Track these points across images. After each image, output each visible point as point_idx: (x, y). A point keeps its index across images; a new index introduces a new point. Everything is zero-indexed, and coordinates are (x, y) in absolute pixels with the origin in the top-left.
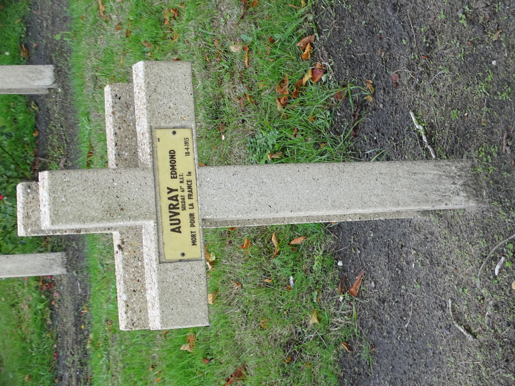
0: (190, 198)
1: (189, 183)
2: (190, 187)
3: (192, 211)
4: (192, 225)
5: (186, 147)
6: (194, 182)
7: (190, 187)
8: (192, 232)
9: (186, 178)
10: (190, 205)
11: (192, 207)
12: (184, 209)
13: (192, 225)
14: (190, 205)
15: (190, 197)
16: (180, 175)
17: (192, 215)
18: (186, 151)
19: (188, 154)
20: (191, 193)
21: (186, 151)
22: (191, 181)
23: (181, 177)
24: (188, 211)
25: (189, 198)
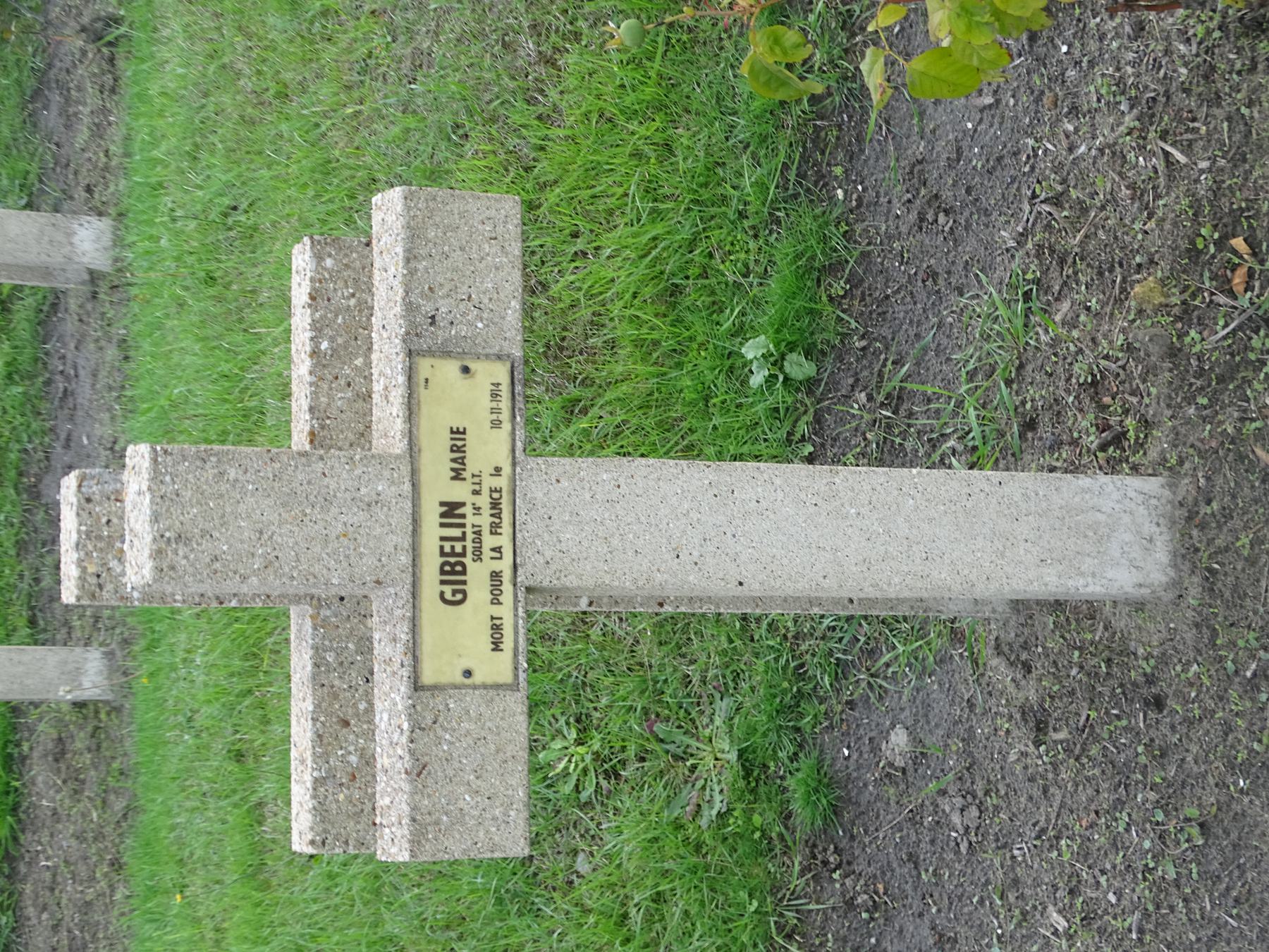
0: (496, 533)
1: (496, 495)
2: (495, 505)
3: (497, 565)
4: (496, 601)
5: (494, 405)
6: (504, 494)
7: (495, 505)
8: (492, 618)
9: (488, 482)
10: (493, 550)
11: (498, 555)
12: (478, 557)
13: (496, 601)
14: (493, 550)
16: (473, 476)
17: (496, 576)
19: (496, 424)
20: (497, 521)
21: (494, 417)
22: (500, 491)
23: (476, 480)
24: (489, 565)
25: (491, 533)
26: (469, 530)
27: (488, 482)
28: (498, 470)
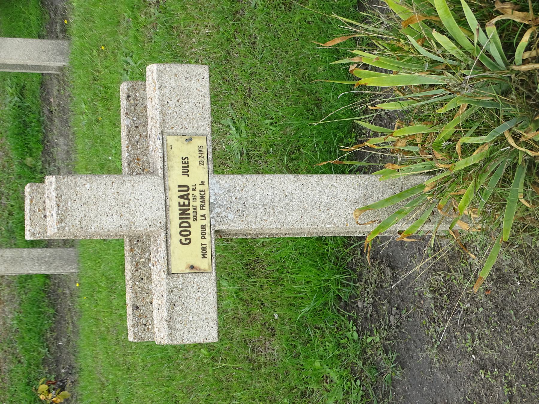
0: (203, 209)
2: (202, 197)
3: (204, 223)
4: (203, 237)
5: (200, 155)
6: (207, 193)
7: (202, 197)
8: (202, 244)
9: (199, 188)
10: (202, 216)
12: (195, 219)
15: (202, 207)
18: (200, 159)
19: (201, 163)
20: (203, 204)
22: (204, 191)
24: (200, 222)
26: (191, 207)
27: (199, 188)
28: (203, 183)
